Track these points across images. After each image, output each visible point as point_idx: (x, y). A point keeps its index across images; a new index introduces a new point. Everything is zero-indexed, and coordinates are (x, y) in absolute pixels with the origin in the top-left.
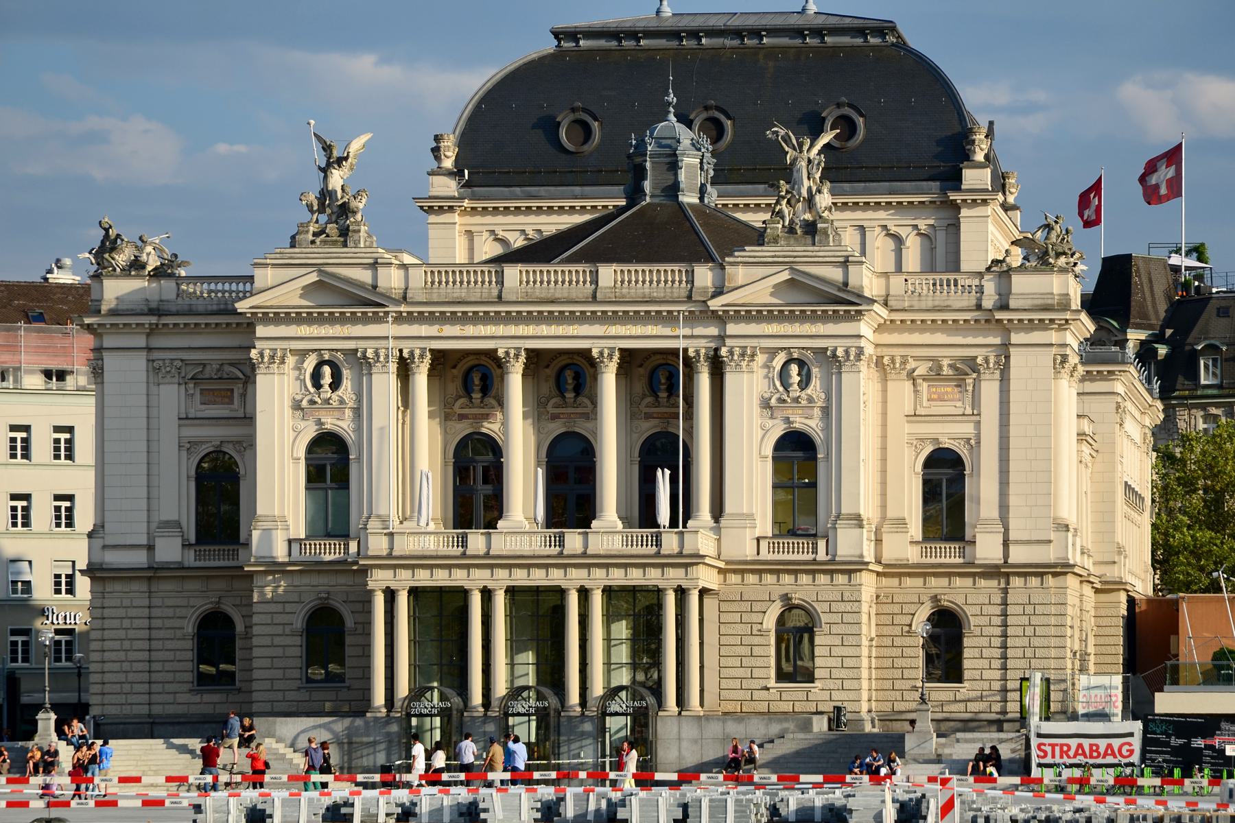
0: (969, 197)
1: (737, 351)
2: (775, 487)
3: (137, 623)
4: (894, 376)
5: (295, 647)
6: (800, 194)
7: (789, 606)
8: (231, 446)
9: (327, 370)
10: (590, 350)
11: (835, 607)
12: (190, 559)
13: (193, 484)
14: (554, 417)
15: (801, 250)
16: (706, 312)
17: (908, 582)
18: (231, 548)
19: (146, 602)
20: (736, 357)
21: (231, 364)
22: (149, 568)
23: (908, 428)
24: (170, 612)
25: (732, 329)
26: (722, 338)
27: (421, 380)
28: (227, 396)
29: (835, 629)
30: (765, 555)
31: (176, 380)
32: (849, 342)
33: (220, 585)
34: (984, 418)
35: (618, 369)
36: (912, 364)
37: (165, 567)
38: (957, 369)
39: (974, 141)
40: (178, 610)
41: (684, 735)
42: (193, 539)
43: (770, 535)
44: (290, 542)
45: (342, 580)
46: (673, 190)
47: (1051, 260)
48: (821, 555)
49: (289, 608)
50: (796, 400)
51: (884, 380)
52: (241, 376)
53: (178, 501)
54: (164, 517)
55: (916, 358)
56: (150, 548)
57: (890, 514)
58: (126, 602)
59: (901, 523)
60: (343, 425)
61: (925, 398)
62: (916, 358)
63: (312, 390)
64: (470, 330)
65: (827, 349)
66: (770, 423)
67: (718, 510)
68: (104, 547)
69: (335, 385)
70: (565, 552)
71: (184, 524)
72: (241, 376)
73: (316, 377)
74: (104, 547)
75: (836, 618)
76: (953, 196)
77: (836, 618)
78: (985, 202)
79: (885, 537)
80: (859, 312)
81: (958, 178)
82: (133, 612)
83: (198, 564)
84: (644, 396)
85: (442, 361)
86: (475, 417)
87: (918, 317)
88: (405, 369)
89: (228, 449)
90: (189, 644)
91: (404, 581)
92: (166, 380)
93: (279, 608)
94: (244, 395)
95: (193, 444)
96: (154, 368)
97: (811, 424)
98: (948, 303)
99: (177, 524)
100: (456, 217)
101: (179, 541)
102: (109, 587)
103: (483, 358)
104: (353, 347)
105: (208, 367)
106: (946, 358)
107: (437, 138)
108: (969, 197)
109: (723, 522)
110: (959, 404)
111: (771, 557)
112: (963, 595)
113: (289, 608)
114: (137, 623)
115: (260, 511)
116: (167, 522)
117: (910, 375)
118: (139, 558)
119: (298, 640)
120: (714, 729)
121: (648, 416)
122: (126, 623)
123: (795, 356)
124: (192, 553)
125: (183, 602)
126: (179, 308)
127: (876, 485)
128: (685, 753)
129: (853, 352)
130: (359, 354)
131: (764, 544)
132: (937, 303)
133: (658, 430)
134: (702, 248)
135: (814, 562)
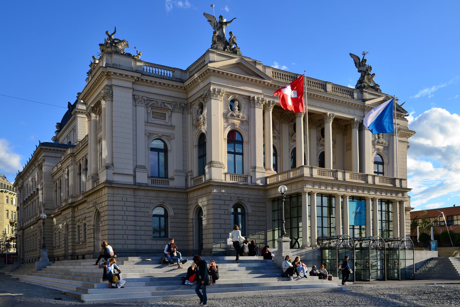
3: (129, 209)
8: (165, 137)
22: (135, 184)
37: (140, 185)
40: (146, 204)
45: (246, 192)
49: (227, 203)
56: (135, 177)
68: (114, 173)
71: (147, 167)
74: (114, 173)
82: (127, 204)
83: (153, 185)
93: (222, 202)
99: (144, 167)
101: (146, 174)
113: (227, 203)
114: (129, 209)
116: (140, 166)
118: (130, 180)
125: (149, 201)
130: (251, 99)
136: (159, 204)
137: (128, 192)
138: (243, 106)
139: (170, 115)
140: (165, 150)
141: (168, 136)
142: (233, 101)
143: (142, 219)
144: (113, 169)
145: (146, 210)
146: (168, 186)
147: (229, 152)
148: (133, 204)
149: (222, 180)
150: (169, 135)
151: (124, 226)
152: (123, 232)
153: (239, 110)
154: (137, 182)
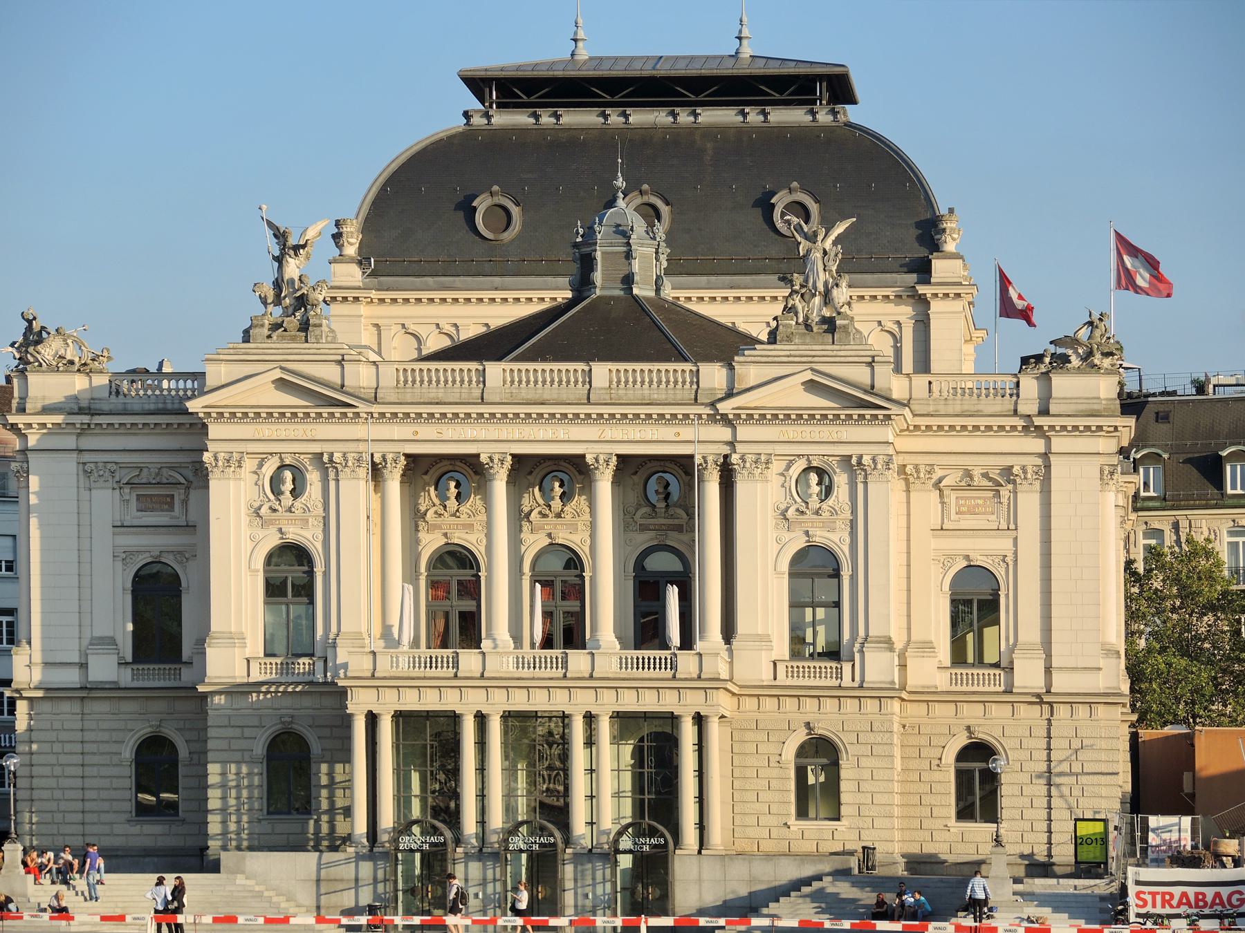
0: (941, 291)
1: (749, 458)
2: (791, 606)
3: (68, 747)
4: (918, 485)
6: (815, 288)
9: (288, 475)
10: (583, 456)
12: (126, 677)
13: (129, 598)
15: (820, 348)
16: (714, 415)
17: (938, 709)
18: (173, 666)
19: (78, 725)
20: (748, 465)
21: (171, 468)
23: (935, 543)
24: (105, 736)
25: (744, 432)
26: (732, 444)
27: (394, 485)
28: (168, 503)
30: (782, 679)
31: (110, 484)
32: (875, 449)
33: (160, 706)
34: (1021, 534)
35: (614, 476)
36: (939, 473)
39: (944, 230)
42: (130, 659)
43: (787, 658)
45: (307, 702)
46: (628, 280)
47: (1097, 362)
49: (247, 732)
50: (817, 513)
51: (908, 491)
52: (183, 481)
54: (97, 633)
55: (942, 467)
57: (913, 639)
58: (57, 725)
59: (927, 647)
61: (953, 512)
62: (942, 467)
63: (271, 497)
64: (450, 431)
65: (851, 456)
66: (787, 536)
67: (728, 632)
69: (295, 493)
70: (568, 675)
71: (119, 640)
72: (183, 481)
73: (276, 482)
76: (922, 289)
78: (958, 295)
79: (909, 663)
80: (888, 417)
81: (923, 270)
82: (64, 736)
83: (136, 684)
84: (639, 507)
87: (946, 422)
88: (377, 472)
91: (387, 705)
92: (101, 483)
94: (185, 502)
95: (129, 554)
96: (85, 471)
97: (837, 540)
98: (980, 407)
99: (112, 641)
100: (363, 309)
101: (114, 659)
103: (458, 463)
104: (319, 451)
105: (145, 470)
106: (978, 466)
107: (338, 224)
108: (941, 291)
109: (735, 643)
111: (789, 682)
113: (247, 732)
114: (68, 747)
115: (215, 626)
117: (937, 485)
118: (71, 677)
121: (644, 528)
122: (57, 748)
123: (815, 464)
124: (129, 671)
126: (112, 406)
127: (904, 604)
129: (880, 460)
131: (781, 668)
132: (966, 407)
134: (669, 346)
136: (149, 730)
137: (65, 707)
139: (183, 497)
141: (179, 552)
142: (282, 467)
143: (104, 771)
145: (114, 748)
146: (176, 684)
148: (78, 736)
149: (234, 677)
150: (181, 549)
151: (55, 792)
153: (292, 491)
154: (90, 679)
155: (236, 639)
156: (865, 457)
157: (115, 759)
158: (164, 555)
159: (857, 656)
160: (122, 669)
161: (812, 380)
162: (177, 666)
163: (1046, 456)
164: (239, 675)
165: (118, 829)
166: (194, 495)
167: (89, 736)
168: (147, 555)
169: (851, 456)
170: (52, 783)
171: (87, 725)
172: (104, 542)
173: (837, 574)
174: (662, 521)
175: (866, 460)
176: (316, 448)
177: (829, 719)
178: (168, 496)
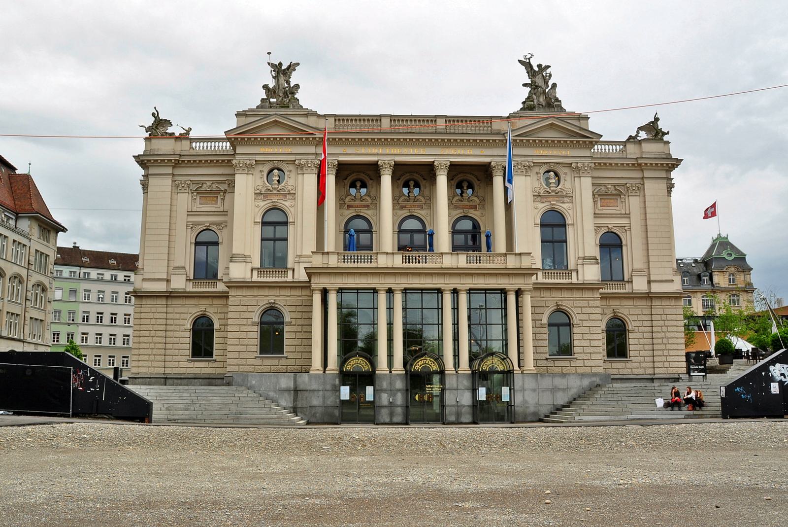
2: (542, 242)
5: (254, 334)
7: (559, 310)
11: (585, 310)
12: (190, 288)
13: (193, 247)
14: (402, 207)
29: (585, 324)
38: (616, 189)
41: (526, 386)
42: (192, 278)
44: (252, 270)
48: (574, 280)
53: (185, 256)
54: (177, 264)
56: (168, 281)
58: (154, 310)
60: (286, 204)
61: (599, 206)
64: (363, 150)
65: (571, 164)
66: (541, 205)
68: (143, 280)
74: (143, 280)
75: (585, 317)
77: (585, 317)
85: (344, 171)
86: (357, 206)
89: (214, 228)
90: (189, 334)
93: (245, 308)
94: (223, 200)
95: (195, 224)
97: (564, 207)
102: (145, 301)
105: (204, 185)
110: (617, 208)
112: (627, 310)
116: (178, 267)
118: (161, 287)
119: (257, 328)
120: (546, 382)
121: (457, 207)
128: (527, 398)
131: (540, 274)
133: (463, 215)
135: (571, 284)
138: (287, 173)
140: (216, 244)
141: (219, 224)
144: (143, 274)
145: (182, 322)
147: (262, 240)
152: (149, 352)
155: (244, 258)
156: (579, 164)
157: (182, 328)
158: (212, 226)
159: (580, 268)
160: (188, 283)
161: (552, 124)
162: (215, 281)
163: (643, 178)
164: (248, 277)
165: (182, 364)
166: (227, 196)
167: (169, 316)
168: (204, 226)
169: (571, 164)
170: (150, 340)
171: (170, 310)
172: (181, 220)
173: (564, 225)
174: (466, 203)
175: (579, 165)
176: (292, 158)
177: (568, 301)
178: (215, 197)
